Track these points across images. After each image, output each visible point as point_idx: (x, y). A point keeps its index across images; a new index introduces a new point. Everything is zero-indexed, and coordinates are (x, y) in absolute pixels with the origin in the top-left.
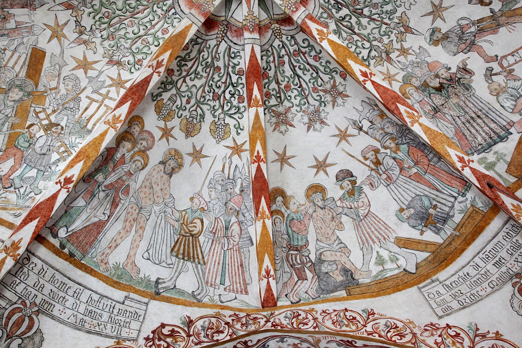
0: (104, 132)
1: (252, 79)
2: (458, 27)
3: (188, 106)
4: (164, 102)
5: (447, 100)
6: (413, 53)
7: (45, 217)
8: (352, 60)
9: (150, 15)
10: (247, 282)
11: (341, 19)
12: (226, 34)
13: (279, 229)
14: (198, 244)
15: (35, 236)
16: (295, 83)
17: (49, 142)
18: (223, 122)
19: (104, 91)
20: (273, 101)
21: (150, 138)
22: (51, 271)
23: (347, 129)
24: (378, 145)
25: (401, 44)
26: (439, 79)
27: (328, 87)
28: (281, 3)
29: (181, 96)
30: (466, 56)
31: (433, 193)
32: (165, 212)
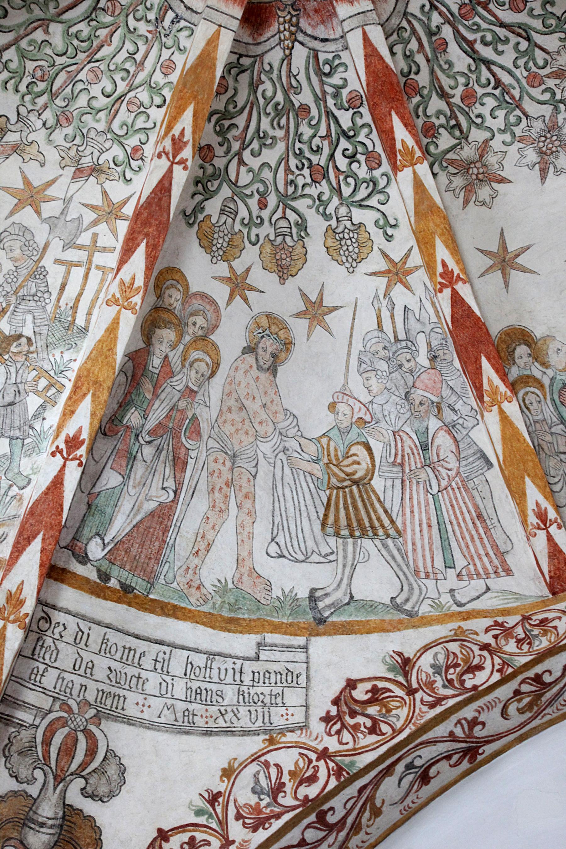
0: (113, 323)
1: (384, 107)
3: (265, 214)
4: (214, 220)
7: (52, 528)
9: (127, 42)
10: (502, 548)
12: (297, 25)
13: (540, 417)
14: (373, 498)
15: (45, 571)
16: (483, 80)
17: (14, 375)
18: (348, 224)
19: (85, 239)
21: (208, 307)
22: (97, 633)
29: (244, 198)
32: (285, 449)
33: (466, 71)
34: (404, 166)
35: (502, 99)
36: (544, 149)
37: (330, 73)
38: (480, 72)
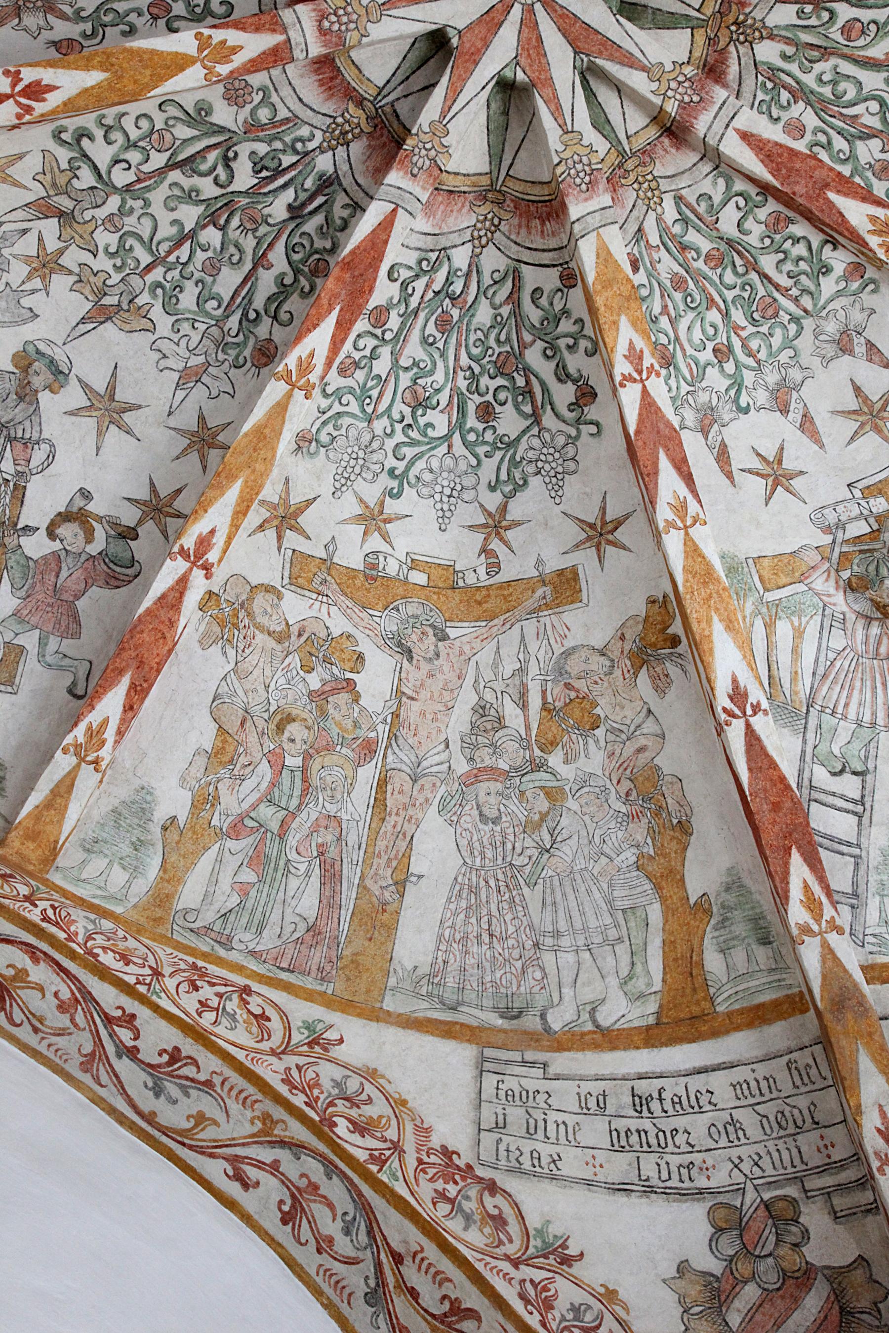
2: (35, 436)
6: (28, 286)
8: (99, 85)
11: (231, 154)
25: (70, 272)
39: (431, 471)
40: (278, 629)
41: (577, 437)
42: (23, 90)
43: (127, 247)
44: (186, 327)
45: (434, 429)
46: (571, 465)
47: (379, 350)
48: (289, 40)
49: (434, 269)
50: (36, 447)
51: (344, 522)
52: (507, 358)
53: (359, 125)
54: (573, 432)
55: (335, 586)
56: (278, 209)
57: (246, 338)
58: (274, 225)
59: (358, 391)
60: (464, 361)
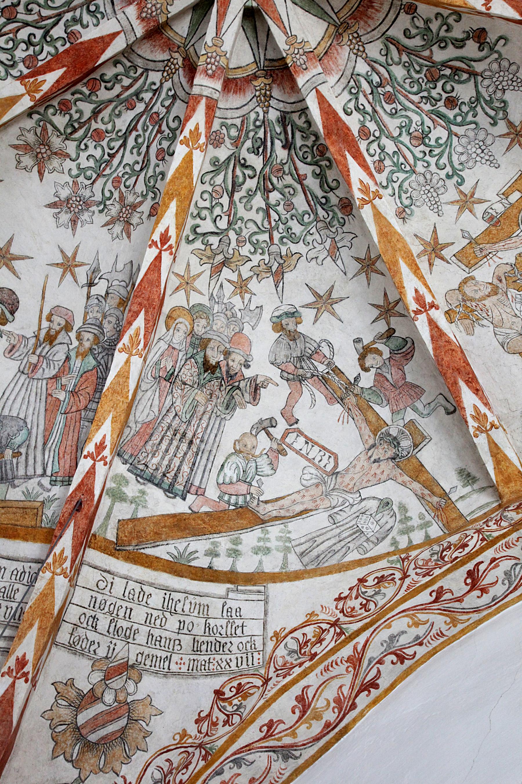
1: (67, 60)
2: (315, 345)
5: (196, 386)
6: (246, 301)
8: (178, 206)
11: (242, 162)
16: (112, 144)
20: (60, 121)
23: (82, 264)
24: (78, 323)
25: (251, 277)
26: (225, 359)
27: (130, 199)
28: (210, 44)
30: (278, 379)
31: (39, 439)
33: (116, 129)
34: (25, 86)
35: (102, 161)
36: (71, 202)
37: (90, 11)
38: (118, 140)
39: (462, 154)
40: (489, 290)
41: (500, 55)
42: (161, 244)
43: (256, 242)
44: (309, 238)
45: (441, 138)
46: (514, 68)
47: (381, 143)
48: (207, 96)
49: (358, 86)
50: (321, 348)
51: (457, 219)
52: (430, 72)
53: (265, 84)
54: (496, 56)
55: (488, 245)
56: (281, 154)
57: (332, 211)
58: (288, 161)
59: (395, 168)
60: (416, 98)
